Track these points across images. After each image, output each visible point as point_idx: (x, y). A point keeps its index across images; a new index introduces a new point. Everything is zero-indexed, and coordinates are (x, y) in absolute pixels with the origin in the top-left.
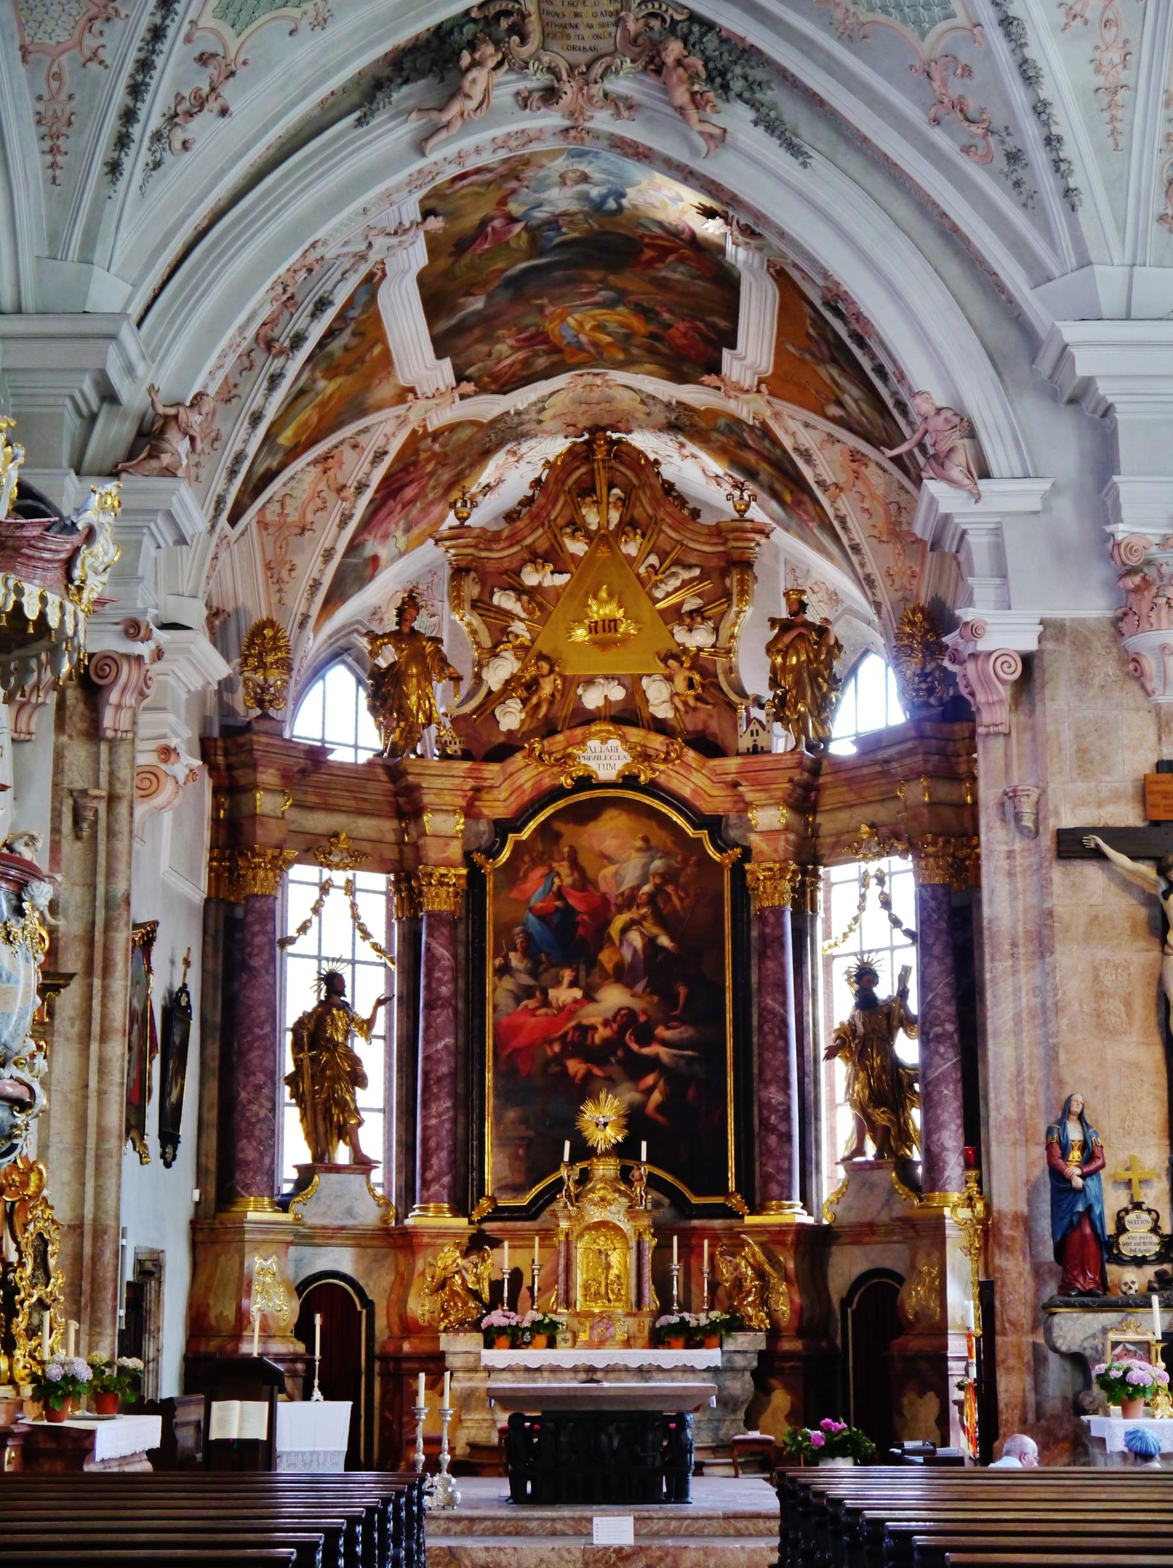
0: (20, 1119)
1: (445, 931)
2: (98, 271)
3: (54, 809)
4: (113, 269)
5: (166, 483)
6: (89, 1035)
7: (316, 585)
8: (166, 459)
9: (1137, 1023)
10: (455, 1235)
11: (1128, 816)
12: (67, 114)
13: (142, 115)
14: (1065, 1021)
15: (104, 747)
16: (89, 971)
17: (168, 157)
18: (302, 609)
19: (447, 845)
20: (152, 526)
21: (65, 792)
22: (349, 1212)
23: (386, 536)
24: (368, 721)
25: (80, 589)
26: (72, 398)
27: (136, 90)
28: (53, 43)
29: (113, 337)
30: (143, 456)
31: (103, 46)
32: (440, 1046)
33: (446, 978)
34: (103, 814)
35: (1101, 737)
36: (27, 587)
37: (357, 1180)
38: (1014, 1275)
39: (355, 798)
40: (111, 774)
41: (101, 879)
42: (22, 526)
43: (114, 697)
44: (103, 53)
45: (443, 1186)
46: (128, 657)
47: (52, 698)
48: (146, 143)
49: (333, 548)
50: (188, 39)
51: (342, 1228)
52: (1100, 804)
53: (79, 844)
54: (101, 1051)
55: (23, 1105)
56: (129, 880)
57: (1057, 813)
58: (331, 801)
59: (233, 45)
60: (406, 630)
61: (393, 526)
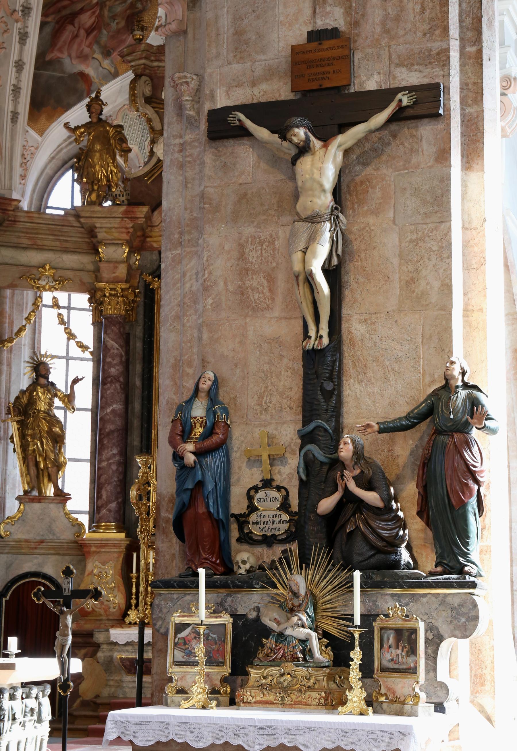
1: (115, 329)
7: (16, 90)
9: (279, 299)
10: (115, 546)
14: (210, 301)
18: (11, 108)
19: (116, 267)
22: (50, 530)
23: (83, 57)
24: (77, 187)
32: (109, 410)
33: (115, 362)
35: (258, 17)
37: (53, 509)
38: (167, 557)
39: (59, 240)
45: (110, 511)
49: (20, 60)
51: (42, 542)
52: (253, 84)
57: (212, 97)
58: (39, 242)
60: (95, 120)
61: (87, 50)
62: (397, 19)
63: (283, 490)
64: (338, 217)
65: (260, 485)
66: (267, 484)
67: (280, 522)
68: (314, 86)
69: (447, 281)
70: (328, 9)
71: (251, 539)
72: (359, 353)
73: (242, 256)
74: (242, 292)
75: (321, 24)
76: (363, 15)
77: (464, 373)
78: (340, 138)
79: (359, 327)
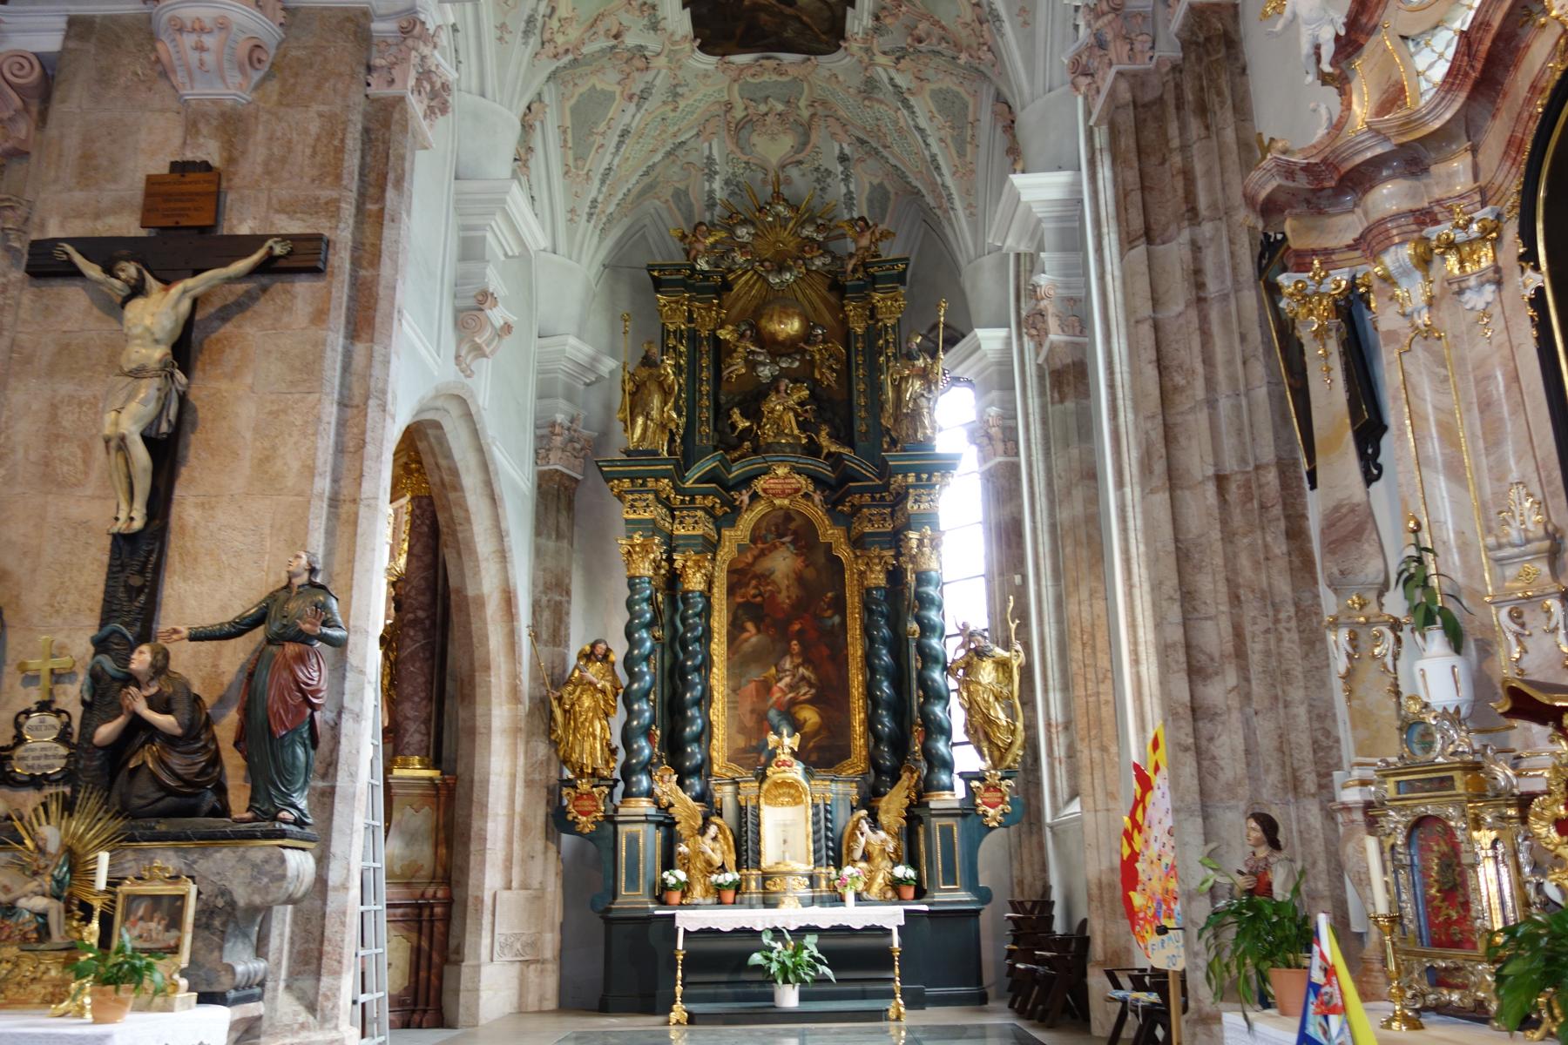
11: (128, 225)
52: (97, 216)
57: (42, 226)
62: (283, 160)
63: (64, 717)
64: (172, 375)
65: (34, 707)
66: (44, 706)
67: (55, 756)
68: (170, 222)
69: (310, 462)
70: (202, 140)
71: (14, 779)
72: (189, 544)
73: (53, 418)
74: (46, 462)
75: (189, 156)
76: (243, 153)
77: (312, 571)
78: (189, 282)
79: (192, 511)
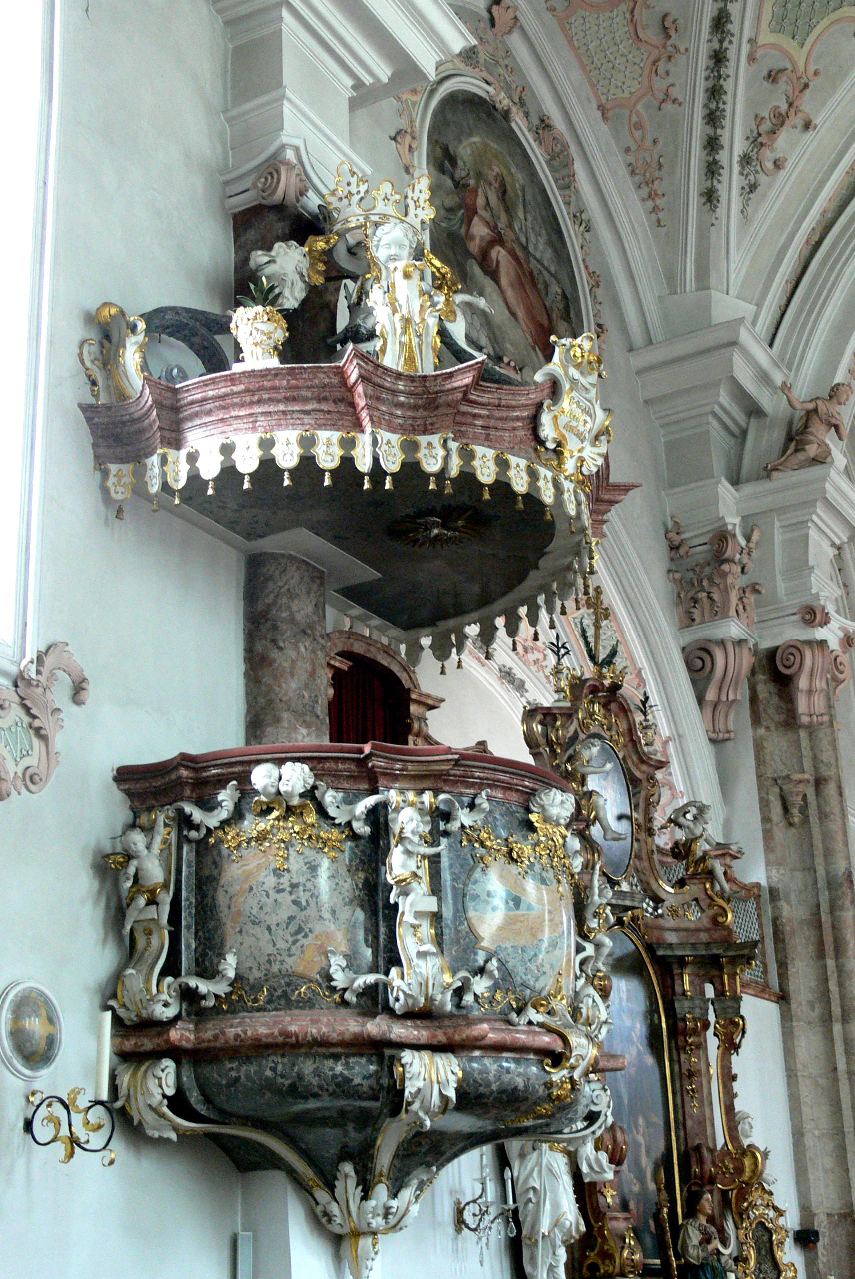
0: (558, 1075)
2: (716, 295)
3: (761, 800)
4: (731, 292)
5: (817, 470)
6: (830, 1017)
8: (812, 450)
12: (656, 157)
13: (725, 141)
15: (803, 734)
16: (821, 954)
17: (762, 179)
20: (814, 517)
21: (770, 782)
25: (558, 452)
26: (714, 414)
27: (713, 118)
28: (626, 95)
29: (734, 343)
30: (789, 452)
31: (672, 85)
34: (811, 798)
36: (479, 450)
40: (815, 758)
41: (819, 861)
42: (451, 375)
43: (803, 683)
44: (675, 92)
46: (809, 643)
47: (742, 694)
48: (736, 168)
50: (751, 59)
53: (793, 830)
54: (843, 1029)
55: (557, 1059)
56: (848, 858)
59: (800, 57)
